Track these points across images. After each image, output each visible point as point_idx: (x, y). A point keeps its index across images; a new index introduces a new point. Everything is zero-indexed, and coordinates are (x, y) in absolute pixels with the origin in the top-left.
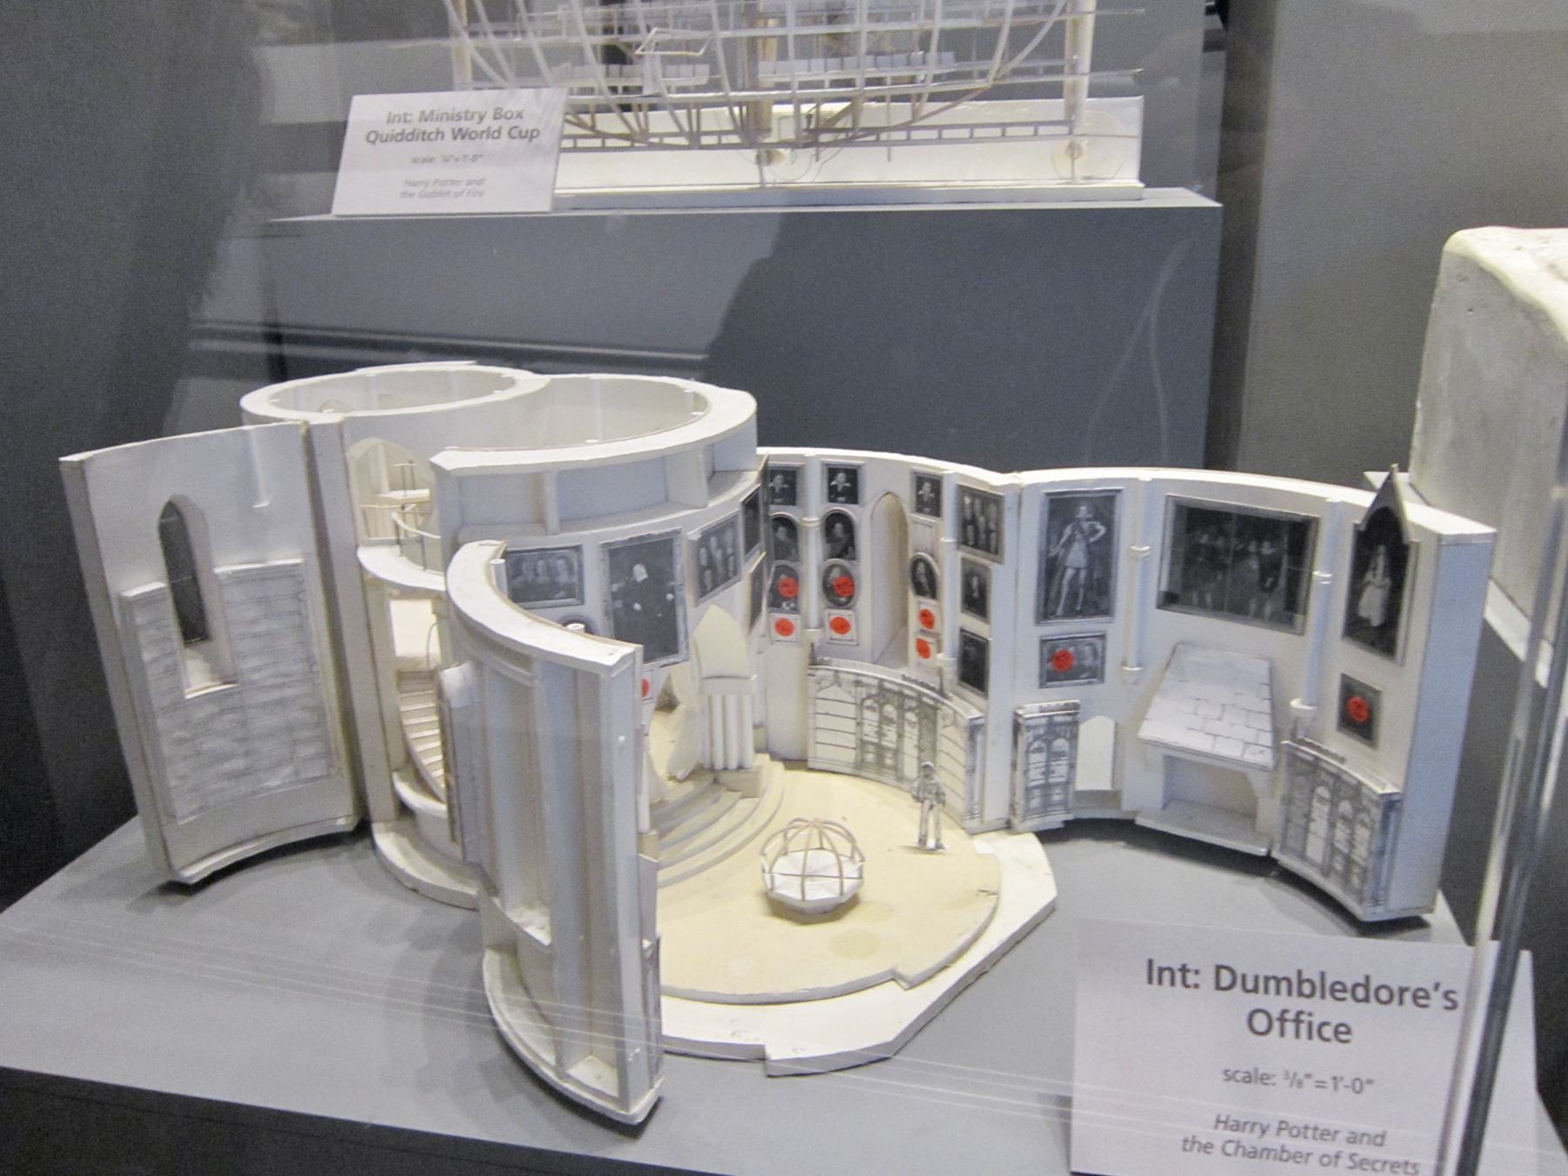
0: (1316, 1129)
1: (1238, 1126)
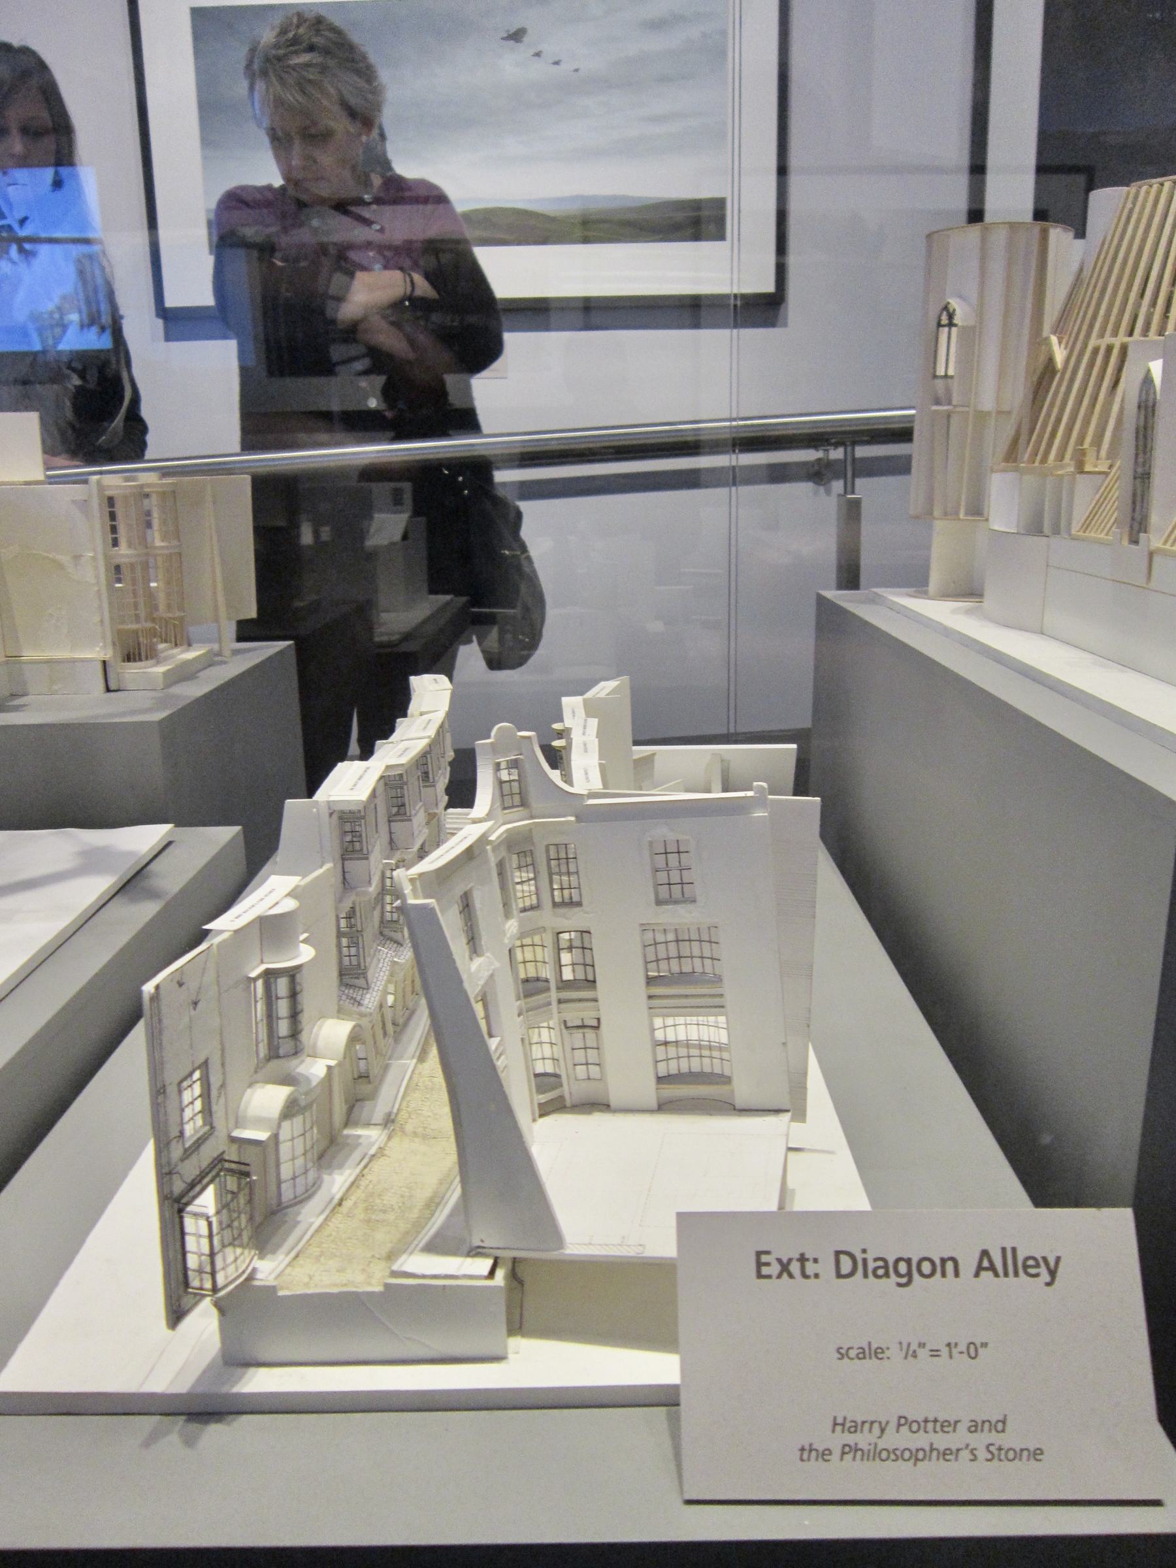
0: (936, 1421)
1: (855, 1428)
